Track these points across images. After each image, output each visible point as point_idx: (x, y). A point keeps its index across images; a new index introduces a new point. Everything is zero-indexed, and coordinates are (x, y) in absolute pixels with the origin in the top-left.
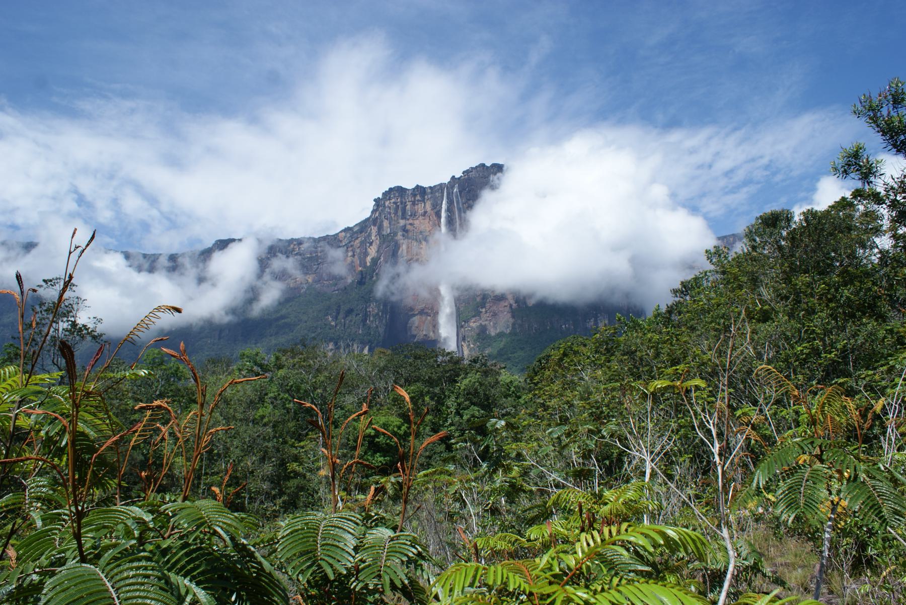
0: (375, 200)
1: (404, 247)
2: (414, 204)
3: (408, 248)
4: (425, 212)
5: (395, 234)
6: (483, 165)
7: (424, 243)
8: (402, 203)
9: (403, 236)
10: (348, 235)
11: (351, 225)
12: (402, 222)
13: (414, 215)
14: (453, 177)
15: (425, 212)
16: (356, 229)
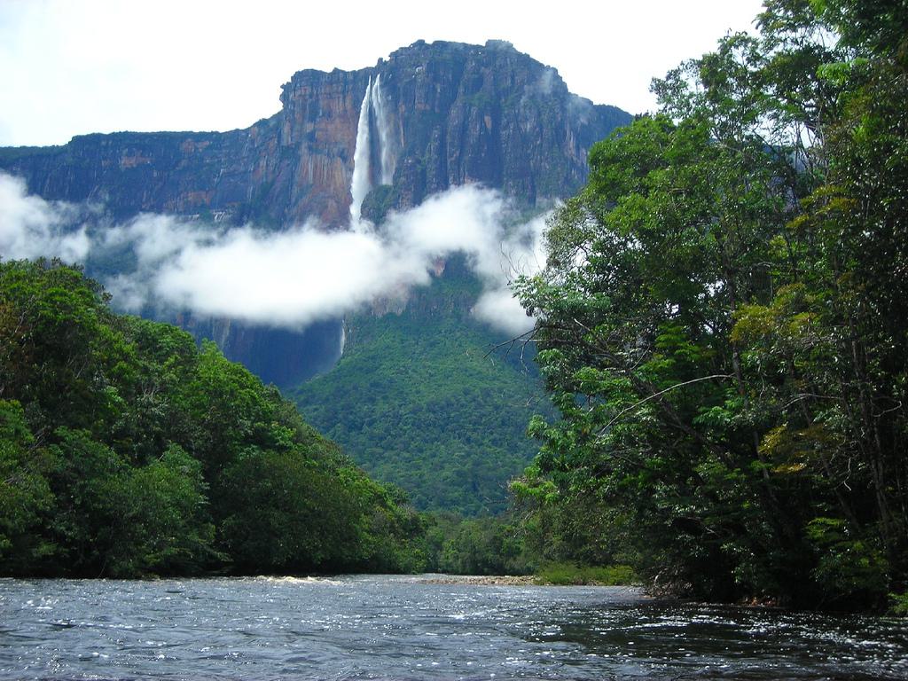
0: (282, 87)
1: (310, 167)
2: (330, 96)
3: (316, 166)
4: (345, 111)
5: (298, 145)
6: (421, 43)
7: (339, 160)
8: (311, 96)
9: (310, 148)
10: (262, 131)
11: (268, 117)
12: (309, 127)
13: (329, 115)
14: (380, 60)
15: (345, 111)
16: (272, 124)
